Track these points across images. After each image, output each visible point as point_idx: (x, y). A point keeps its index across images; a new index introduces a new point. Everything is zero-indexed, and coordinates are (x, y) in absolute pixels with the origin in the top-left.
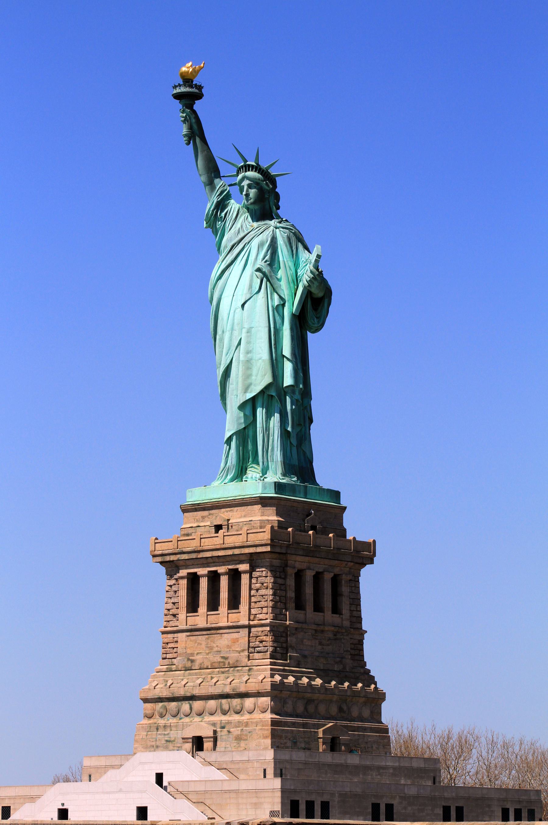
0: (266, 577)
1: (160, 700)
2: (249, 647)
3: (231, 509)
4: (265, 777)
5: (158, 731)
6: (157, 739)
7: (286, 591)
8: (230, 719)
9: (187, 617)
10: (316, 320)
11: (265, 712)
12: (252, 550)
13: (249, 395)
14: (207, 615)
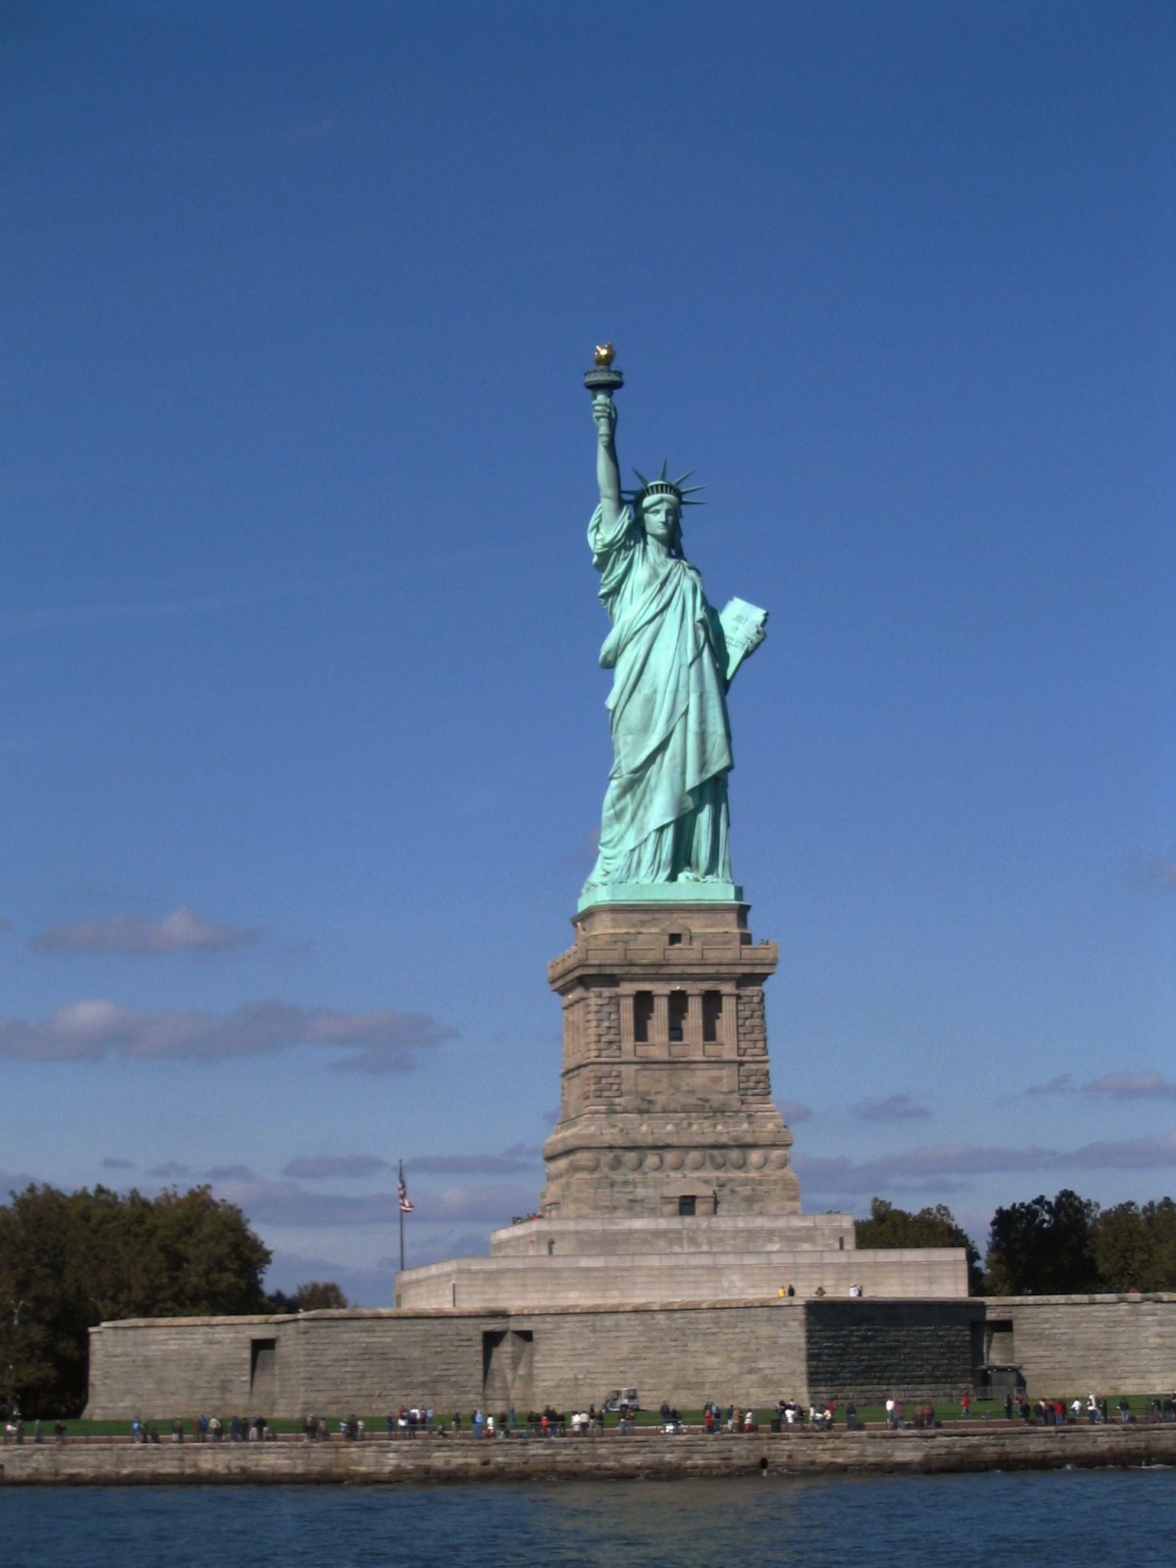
1: (611, 1148)
2: (739, 1089)
4: (842, 1247)
6: (614, 1198)
9: (635, 1046)
12: (747, 970)
14: (670, 1046)
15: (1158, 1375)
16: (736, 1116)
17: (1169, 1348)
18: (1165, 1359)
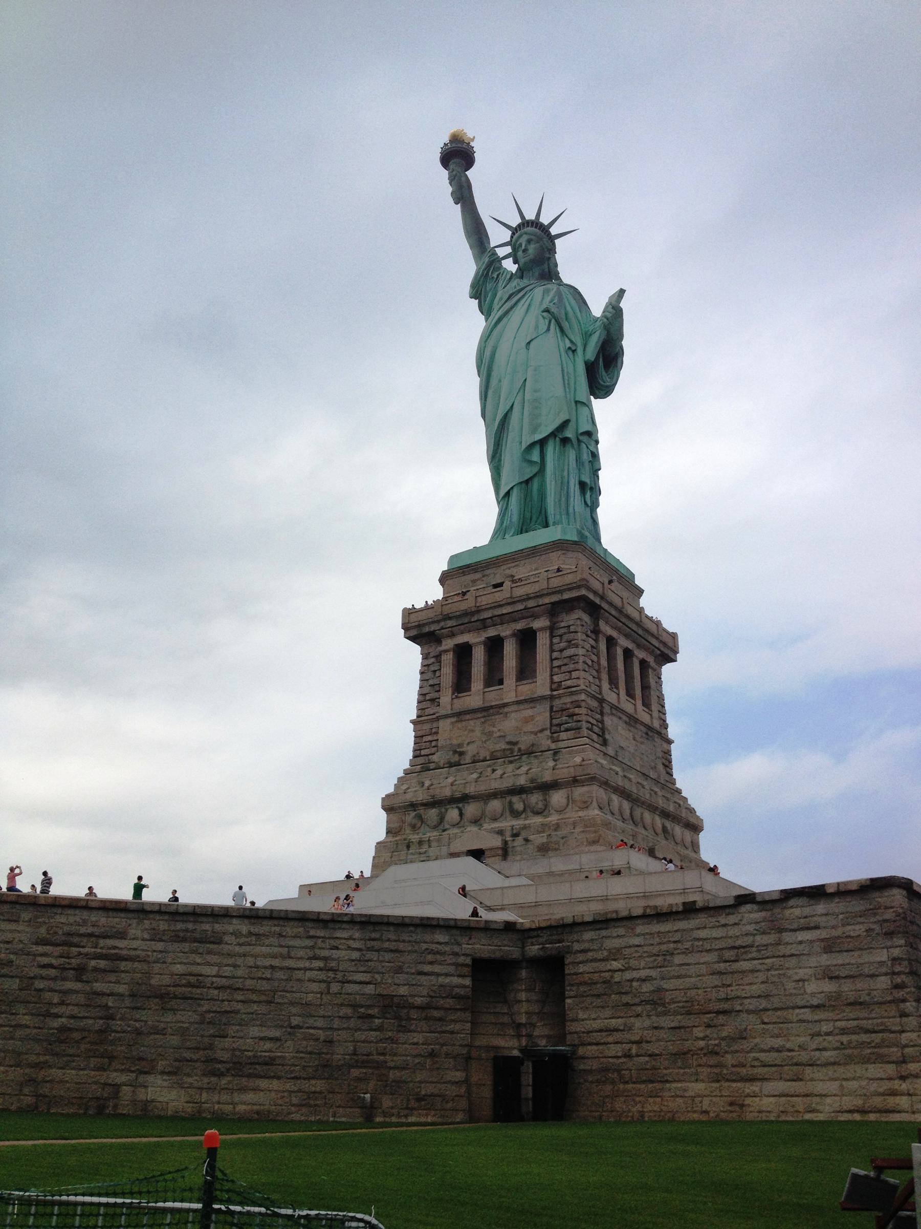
0: (576, 632)
1: (413, 806)
2: (551, 725)
3: (516, 563)
5: (408, 850)
7: (598, 656)
8: (527, 822)
9: (452, 699)
10: (609, 380)
11: (587, 807)
12: (555, 598)
13: (538, 437)
14: (484, 693)
15: (830, 1071)
16: (541, 755)
17: (850, 1004)
18: (844, 1031)
